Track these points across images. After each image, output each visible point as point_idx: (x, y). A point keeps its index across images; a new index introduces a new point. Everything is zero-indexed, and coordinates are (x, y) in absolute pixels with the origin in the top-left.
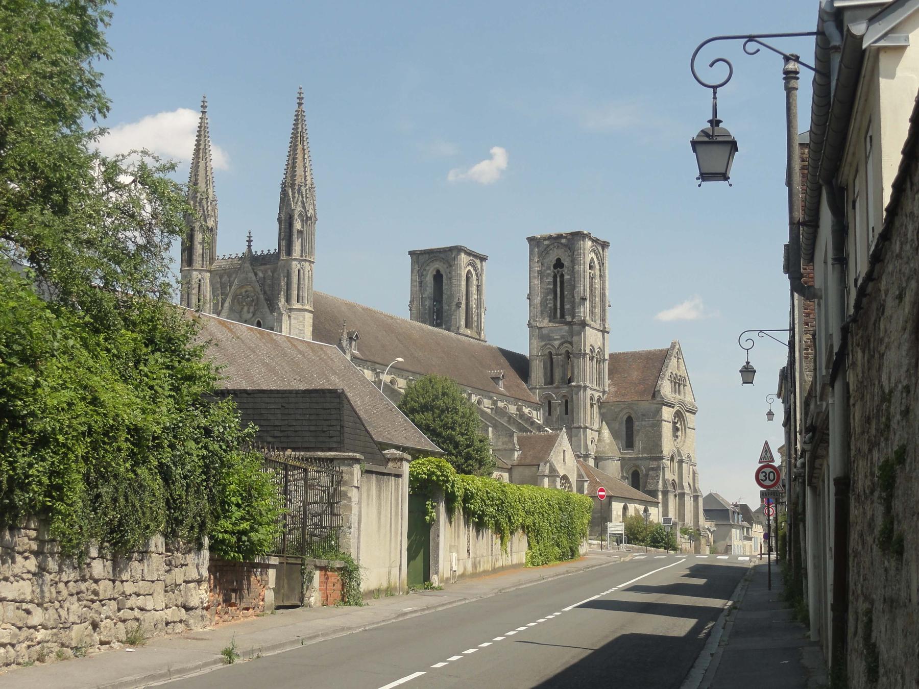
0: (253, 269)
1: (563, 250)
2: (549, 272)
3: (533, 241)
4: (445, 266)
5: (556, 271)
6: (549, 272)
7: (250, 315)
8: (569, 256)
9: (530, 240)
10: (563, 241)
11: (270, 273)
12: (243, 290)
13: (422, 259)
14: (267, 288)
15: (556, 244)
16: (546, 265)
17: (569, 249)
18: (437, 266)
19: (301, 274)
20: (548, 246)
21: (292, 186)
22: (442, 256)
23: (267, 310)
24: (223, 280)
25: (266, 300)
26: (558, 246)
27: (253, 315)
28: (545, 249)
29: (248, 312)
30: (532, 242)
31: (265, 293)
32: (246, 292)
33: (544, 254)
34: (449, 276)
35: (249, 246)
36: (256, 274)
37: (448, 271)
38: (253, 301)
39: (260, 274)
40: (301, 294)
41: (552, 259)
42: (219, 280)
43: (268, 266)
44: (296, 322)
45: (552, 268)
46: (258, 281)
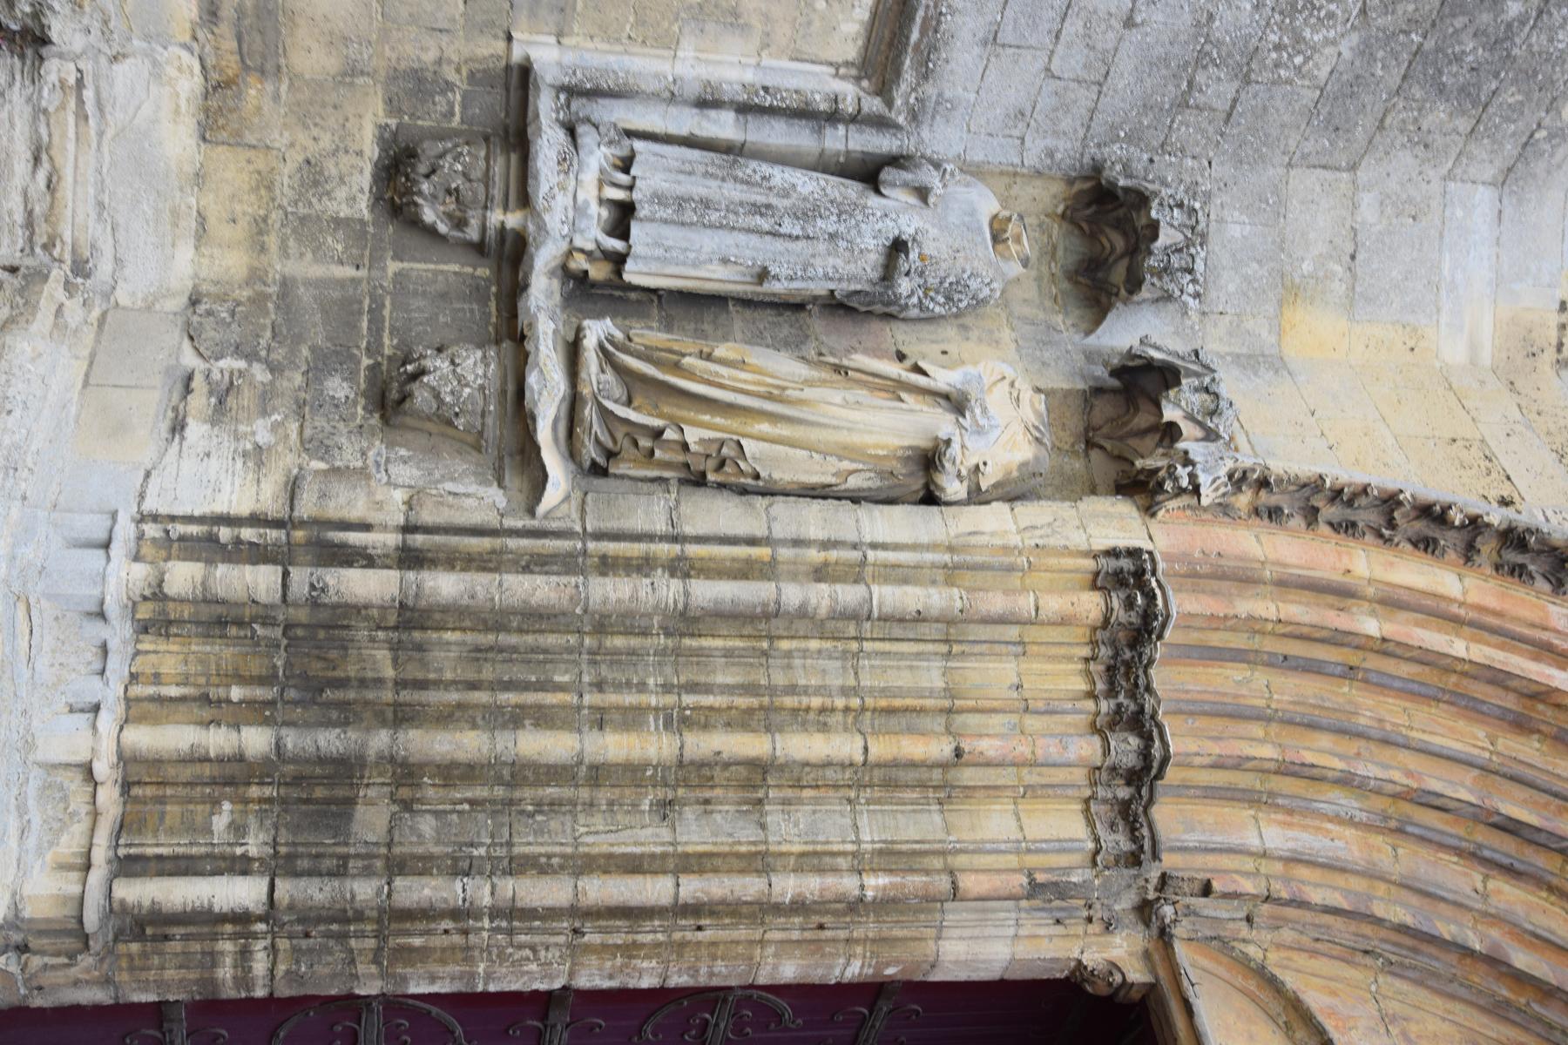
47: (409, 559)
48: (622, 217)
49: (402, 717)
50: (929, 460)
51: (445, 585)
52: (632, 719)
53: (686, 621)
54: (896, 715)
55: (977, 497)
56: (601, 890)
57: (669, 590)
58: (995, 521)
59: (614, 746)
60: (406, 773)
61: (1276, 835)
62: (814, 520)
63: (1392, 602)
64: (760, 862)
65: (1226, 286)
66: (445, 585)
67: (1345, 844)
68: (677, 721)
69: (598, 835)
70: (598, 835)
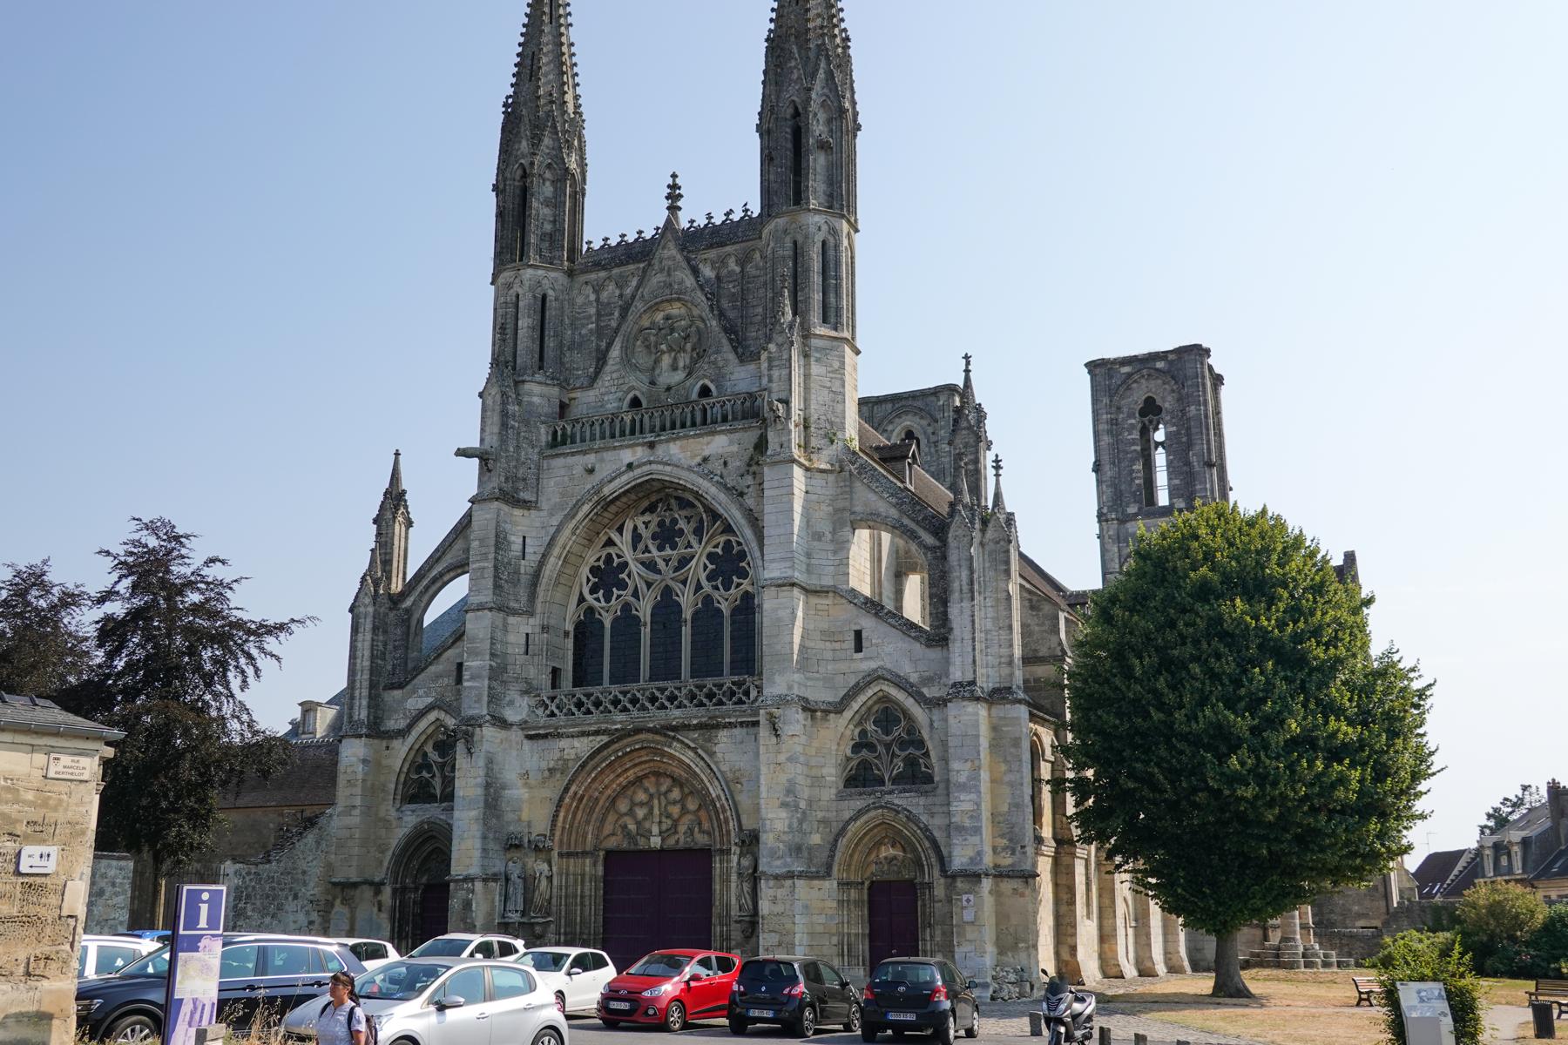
0: (688, 260)
1: (1159, 382)
2: (1133, 421)
3: (1099, 369)
4: (924, 422)
5: (1146, 420)
6: (1133, 421)
7: (680, 376)
8: (1173, 391)
9: (1093, 366)
10: (1160, 365)
11: (733, 265)
12: (659, 317)
13: (879, 412)
14: (725, 304)
15: (1145, 372)
16: (1125, 410)
17: (1173, 377)
18: (908, 423)
19: (831, 253)
20: (1129, 375)
21: (802, 36)
22: (919, 404)
23: (731, 356)
24: (604, 296)
25: (726, 330)
26: (1149, 375)
27: (689, 374)
28: (1124, 382)
29: (674, 368)
30: (1098, 371)
31: (722, 315)
32: (667, 318)
33: (1122, 389)
34: (933, 439)
35: (673, 209)
36: (695, 272)
37: (930, 430)
38: (687, 338)
39: (708, 272)
40: (832, 300)
41: (1138, 396)
42: (592, 297)
43: (728, 249)
44: (822, 370)
45: (1137, 415)
46: (701, 287)
47: (560, 934)
48: (517, 911)
49: (575, 934)
50: (547, 877)
51: (562, 930)
52: (576, 910)
53: (566, 905)
54: (576, 881)
55: (551, 870)
56: (593, 913)
57: (563, 907)
58: (554, 869)
59: (579, 912)
60: (581, 933)
61: (590, 836)
62: (555, 890)
63: (564, 822)
64: (590, 896)
65: (519, 829)
66: (562, 930)
67: (591, 828)
68: (576, 905)
69: (587, 913)
70: (587, 913)
